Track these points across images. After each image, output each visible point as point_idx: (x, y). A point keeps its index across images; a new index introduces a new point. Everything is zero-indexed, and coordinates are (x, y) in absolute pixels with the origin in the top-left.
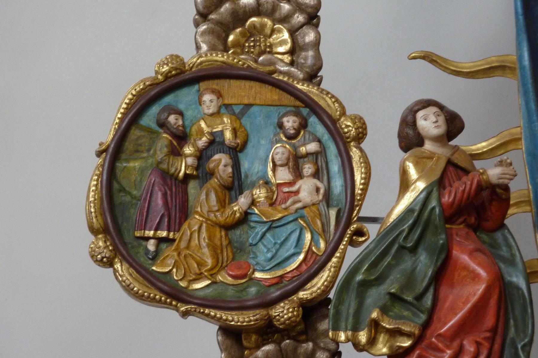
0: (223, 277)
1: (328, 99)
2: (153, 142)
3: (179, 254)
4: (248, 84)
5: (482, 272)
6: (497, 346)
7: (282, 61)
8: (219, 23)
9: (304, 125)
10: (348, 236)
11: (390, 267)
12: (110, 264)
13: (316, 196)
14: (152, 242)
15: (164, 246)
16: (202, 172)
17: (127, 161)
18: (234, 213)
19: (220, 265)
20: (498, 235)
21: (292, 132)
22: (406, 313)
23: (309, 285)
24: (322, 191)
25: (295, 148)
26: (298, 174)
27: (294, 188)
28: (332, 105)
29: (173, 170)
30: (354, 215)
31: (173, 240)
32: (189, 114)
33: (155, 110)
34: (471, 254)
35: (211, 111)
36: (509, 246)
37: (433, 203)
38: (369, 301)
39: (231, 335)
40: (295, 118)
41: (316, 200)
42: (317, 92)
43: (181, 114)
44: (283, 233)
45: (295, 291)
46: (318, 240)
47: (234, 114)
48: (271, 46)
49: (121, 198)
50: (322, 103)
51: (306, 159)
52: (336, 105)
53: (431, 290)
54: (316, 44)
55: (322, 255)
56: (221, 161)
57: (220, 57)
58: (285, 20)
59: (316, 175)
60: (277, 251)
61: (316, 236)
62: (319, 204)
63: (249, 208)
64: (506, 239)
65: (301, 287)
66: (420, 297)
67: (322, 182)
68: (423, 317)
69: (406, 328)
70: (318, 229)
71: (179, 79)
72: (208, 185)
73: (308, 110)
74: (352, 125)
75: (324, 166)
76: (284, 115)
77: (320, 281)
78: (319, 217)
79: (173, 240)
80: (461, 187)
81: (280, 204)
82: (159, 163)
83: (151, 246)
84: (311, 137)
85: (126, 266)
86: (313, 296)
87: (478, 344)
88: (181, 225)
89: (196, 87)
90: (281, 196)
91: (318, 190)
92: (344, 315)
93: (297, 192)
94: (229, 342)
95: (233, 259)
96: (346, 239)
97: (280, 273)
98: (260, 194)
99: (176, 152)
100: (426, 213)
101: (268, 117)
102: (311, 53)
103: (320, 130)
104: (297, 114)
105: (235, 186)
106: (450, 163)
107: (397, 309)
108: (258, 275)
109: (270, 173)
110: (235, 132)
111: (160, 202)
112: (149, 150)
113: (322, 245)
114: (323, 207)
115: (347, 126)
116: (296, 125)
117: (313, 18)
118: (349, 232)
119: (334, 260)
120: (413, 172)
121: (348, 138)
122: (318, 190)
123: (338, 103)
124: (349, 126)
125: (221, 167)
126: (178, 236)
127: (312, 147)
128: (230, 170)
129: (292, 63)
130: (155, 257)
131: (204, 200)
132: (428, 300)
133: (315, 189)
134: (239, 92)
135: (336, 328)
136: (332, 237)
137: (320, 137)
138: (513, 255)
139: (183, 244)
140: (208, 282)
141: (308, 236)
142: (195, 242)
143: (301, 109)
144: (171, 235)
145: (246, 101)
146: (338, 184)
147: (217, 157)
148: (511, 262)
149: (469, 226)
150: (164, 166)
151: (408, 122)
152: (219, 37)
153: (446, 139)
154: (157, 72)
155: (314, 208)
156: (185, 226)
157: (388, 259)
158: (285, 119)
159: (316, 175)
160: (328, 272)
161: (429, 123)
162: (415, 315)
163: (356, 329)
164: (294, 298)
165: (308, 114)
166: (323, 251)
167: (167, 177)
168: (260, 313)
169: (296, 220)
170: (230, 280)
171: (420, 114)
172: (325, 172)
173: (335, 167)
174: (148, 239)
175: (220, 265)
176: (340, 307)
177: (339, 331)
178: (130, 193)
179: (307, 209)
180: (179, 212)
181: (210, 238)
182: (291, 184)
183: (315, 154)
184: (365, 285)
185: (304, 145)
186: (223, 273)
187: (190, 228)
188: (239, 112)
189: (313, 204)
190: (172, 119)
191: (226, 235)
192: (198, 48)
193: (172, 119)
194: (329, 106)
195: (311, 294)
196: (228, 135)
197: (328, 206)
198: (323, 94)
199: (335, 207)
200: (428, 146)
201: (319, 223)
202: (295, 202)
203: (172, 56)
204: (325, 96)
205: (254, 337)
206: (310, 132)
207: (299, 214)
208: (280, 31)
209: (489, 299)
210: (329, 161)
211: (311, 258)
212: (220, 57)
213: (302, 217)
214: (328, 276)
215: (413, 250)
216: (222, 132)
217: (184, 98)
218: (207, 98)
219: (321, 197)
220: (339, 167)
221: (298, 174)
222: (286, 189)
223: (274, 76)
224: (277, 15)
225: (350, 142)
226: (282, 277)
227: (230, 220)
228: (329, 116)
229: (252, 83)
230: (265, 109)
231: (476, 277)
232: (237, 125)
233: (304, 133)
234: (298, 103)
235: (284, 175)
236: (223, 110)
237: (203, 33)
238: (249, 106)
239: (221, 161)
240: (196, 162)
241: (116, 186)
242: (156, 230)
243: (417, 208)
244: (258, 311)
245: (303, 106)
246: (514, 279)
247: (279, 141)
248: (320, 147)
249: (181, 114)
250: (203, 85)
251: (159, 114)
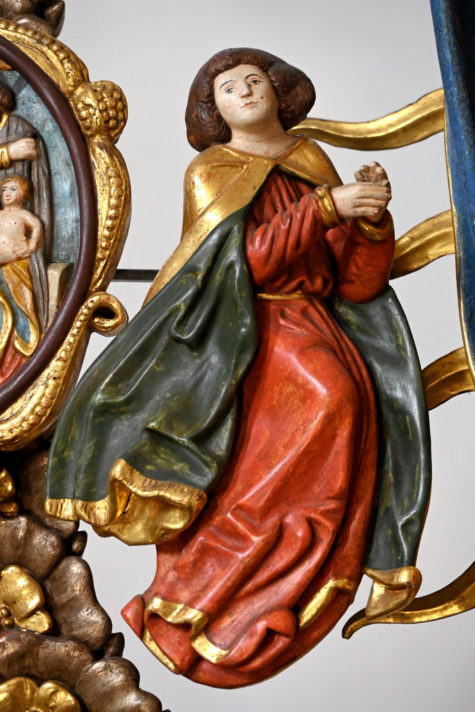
1: (50, 54)
5: (321, 389)
6: (356, 525)
10: (82, 318)
11: (154, 378)
13: (25, 244)
20: (375, 311)
22: (178, 467)
24: (36, 233)
28: (59, 66)
30: (96, 276)
34: (302, 353)
36: (393, 330)
37: (233, 255)
38: (114, 442)
41: (22, 251)
42: (31, 41)
46: (26, 327)
50: (40, 62)
51: (10, 171)
52: (67, 65)
53: (229, 423)
55: (31, 356)
59: (28, 202)
61: (21, 321)
62: (30, 257)
64: (388, 317)
66: (203, 438)
67: (39, 217)
68: (209, 475)
69: (174, 496)
70: (26, 307)
73: (18, 74)
74: (94, 105)
75: (43, 183)
78: (29, 283)
80: (287, 224)
84: (20, 128)
86: (14, 434)
87: (312, 524)
91: (28, 232)
92: (72, 468)
96: (78, 324)
100: (218, 277)
106: (277, 172)
107: (162, 459)
113: (33, 338)
114: (38, 262)
115: (88, 105)
118: (85, 311)
120: (203, 194)
121: (88, 128)
123: (69, 61)
124: (90, 106)
127: (22, 148)
132: (222, 442)
133: (22, 229)
135: (58, 494)
136: (51, 320)
137: (39, 128)
138: (400, 348)
143: (5, 73)
146: (69, 217)
148: (396, 362)
149: (310, 296)
151: (202, 95)
153: (277, 126)
155: (19, 266)
157: (151, 363)
160: (43, 387)
161: (238, 99)
162: (195, 469)
163: (89, 497)
165: (17, 82)
166: (34, 348)
171: (220, 80)
172: (45, 195)
173: (64, 184)
176: (66, 454)
177: (64, 498)
179: (8, 267)
183: (27, 162)
184: (108, 412)
189: (19, 259)
194: (53, 67)
195: (11, 431)
197: (48, 260)
198: (42, 43)
199: (63, 261)
200: (239, 141)
201: (28, 295)
204: (45, 49)
206: (19, 117)
209: (334, 437)
210: (53, 172)
211: (11, 362)
214: (43, 395)
215: (199, 343)
219: (33, 244)
220: (72, 185)
225: (93, 136)
228: (54, 87)
231: (308, 395)
233: (8, 120)
243: (202, 266)
245: (8, 67)
246: (399, 394)
248: (37, 147)
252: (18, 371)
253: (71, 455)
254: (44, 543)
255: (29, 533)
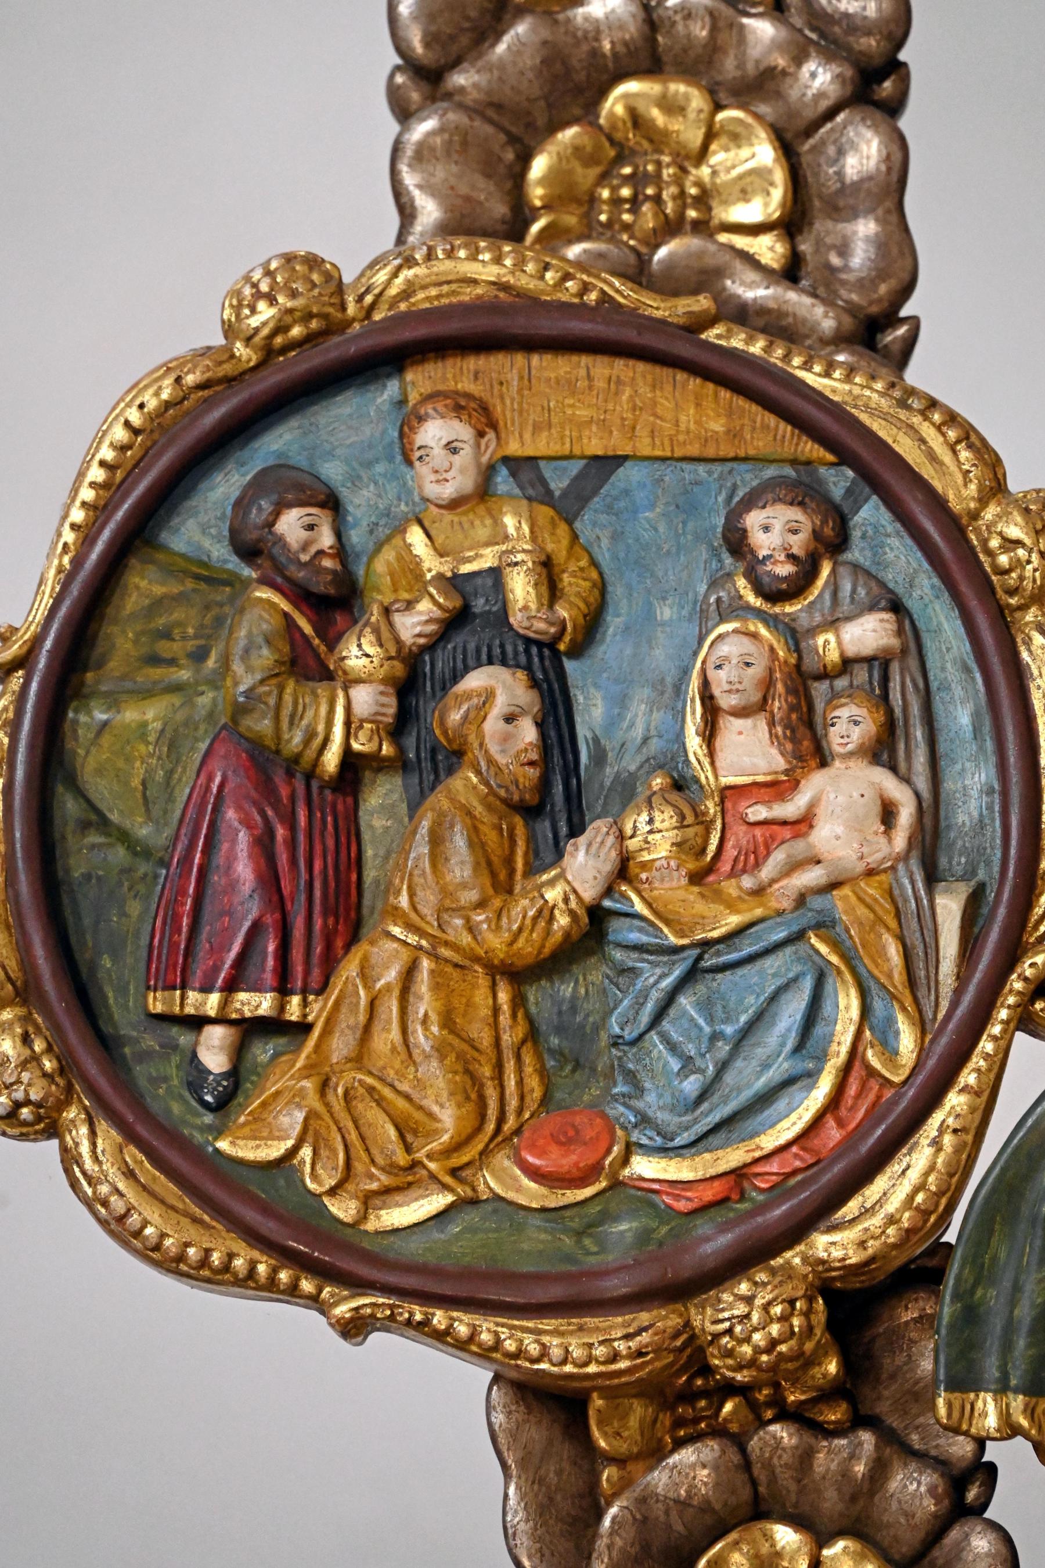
0: (506, 1180)
1: (928, 431)
2: (217, 626)
3: (324, 1086)
4: (602, 368)
7: (750, 259)
8: (491, 108)
9: (833, 540)
10: (1011, 1000)
12: (48, 1125)
13: (883, 840)
14: (216, 1034)
15: (262, 1051)
16: (417, 740)
17: (113, 702)
18: (547, 913)
19: (489, 1129)
21: (785, 569)
23: (852, 1208)
24: (906, 816)
25: (795, 636)
26: (809, 747)
27: (790, 809)
28: (947, 458)
29: (296, 740)
31: (304, 1028)
32: (360, 504)
33: (224, 487)
35: (447, 491)
39: (550, 1407)
40: (795, 514)
41: (879, 856)
42: (884, 403)
43: (331, 503)
44: (744, 990)
45: (798, 1231)
46: (891, 1021)
47: (546, 497)
48: (704, 199)
49: (85, 857)
50: (905, 447)
51: (841, 683)
52: (964, 454)
54: (892, 186)
55: (905, 1082)
56: (493, 704)
57: (484, 268)
58: (760, 86)
59: (883, 750)
60: (723, 1067)
61: (878, 1005)
62: (893, 868)
63: (609, 891)
65: (821, 1213)
67: (907, 780)
70: (890, 976)
71: (321, 357)
72: (439, 799)
73: (850, 473)
74: (1028, 541)
75: (915, 709)
76: (750, 502)
77: (895, 1191)
78: (893, 924)
79: (304, 1028)
81: (733, 874)
82: (239, 711)
83: (214, 1051)
84: (862, 592)
85: (108, 1136)
86: (870, 1251)
88: (330, 964)
89: (392, 388)
90: (739, 836)
91: (888, 814)
93: (804, 823)
94: (536, 1433)
95: (546, 1100)
96: (1003, 1014)
97: (733, 1157)
98: (655, 833)
99: (308, 664)
101: (686, 505)
102: (865, 229)
103: (901, 560)
104: (803, 491)
105: (557, 796)
108: (645, 1167)
109: (694, 743)
110: (548, 575)
111: (244, 870)
112: (199, 656)
113: (907, 1042)
114: (910, 881)
116: (798, 543)
117: (877, 82)
118: (1018, 986)
119: (955, 1100)
121: (1012, 592)
122: (888, 814)
123: (970, 447)
124: (1018, 543)
125: (493, 725)
126: (317, 1009)
127: (867, 633)
128: (528, 732)
129: (791, 272)
130: (228, 1096)
131: (422, 862)
133: (876, 809)
134: (566, 405)
135: (963, 1380)
136: (944, 1005)
137: (900, 590)
139: (340, 1046)
140: (439, 1201)
141: (846, 1005)
142: (386, 1038)
143: (822, 470)
144: (294, 1010)
145: (595, 446)
147: (475, 680)
150: (261, 725)
152: (488, 167)
154: (229, 330)
155: (871, 890)
156: (349, 969)
158: (753, 519)
159: (883, 750)
160: (928, 1151)
164: (793, 1257)
165: (849, 492)
166: (910, 1064)
167: (271, 769)
168: (664, 1319)
169: (798, 937)
170: (530, 1193)
172: (919, 734)
173: (961, 714)
174: (198, 1023)
175: (489, 1129)
176: (979, 1293)
177: (977, 1391)
178: (124, 837)
179: (846, 891)
180: (323, 911)
181: (448, 1022)
182: (778, 788)
183: (880, 663)
185: (833, 623)
186: (503, 1160)
187: (365, 974)
188: (569, 491)
189: (870, 873)
190: (291, 525)
191: (519, 1001)
192: (407, 212)
193: (291, 525)
194: (932, 457)
195: (862, 1244)
196: (521, 588)
197: (932, 878)
198: (908, 408)
199: (963, 878)
201: (893, 952)
202: (794, 867)
203: (289, 259)
204: (916, 420)
205: (638, 1412)
206: (856, 567)
207: (812, 916)
208: (737, 137)
210: (934, 685)
211: (859, 1095)
212: (484, 268)
213: (825, 925)
214: (931, 1168)
216: (496, 574)
217: (339, 433)
218: (434, 433)
219: (900, 840)
220: (976, 716)
221: (809, 747)
222: (759, 812)
223: (712, 335)
224: (729, 67)
225: (1023, 608)
226: (739, 1174)
227: (528, 947)
228: (937, 503)
229: (620, 367)
230: (670, 474)
232: (557, 545)
233: (834, 572)
234: (810, 449)
235: (749, 750)
236: (503, 481)
237: (423, 154)
238: (606, 465)
239: (493, 704)
240: (391, 708)
241: (69, 806)
242: (231, 987)
244: (644, 1317)
245: (830, 458)
247: (735, 609)
248: (900, 632)
249: (331, 503)
250: (419, 379)
251: (242, 505)
252: (874, 1116)
253: (993, 1298)
254: (913, 1489)
255: (879, 1471)
